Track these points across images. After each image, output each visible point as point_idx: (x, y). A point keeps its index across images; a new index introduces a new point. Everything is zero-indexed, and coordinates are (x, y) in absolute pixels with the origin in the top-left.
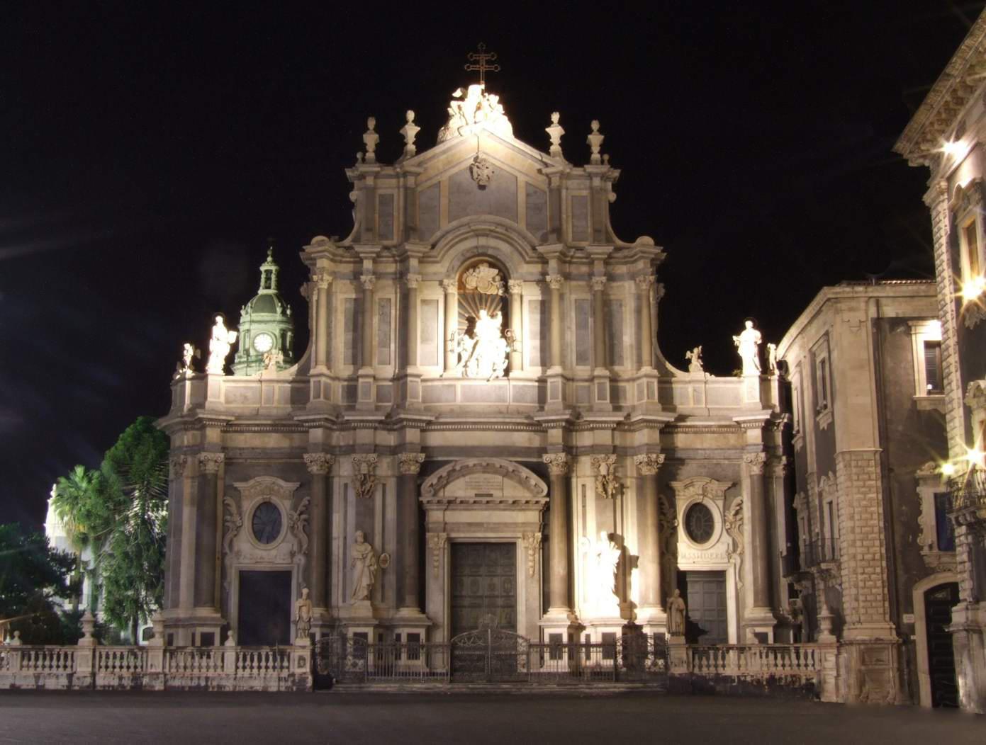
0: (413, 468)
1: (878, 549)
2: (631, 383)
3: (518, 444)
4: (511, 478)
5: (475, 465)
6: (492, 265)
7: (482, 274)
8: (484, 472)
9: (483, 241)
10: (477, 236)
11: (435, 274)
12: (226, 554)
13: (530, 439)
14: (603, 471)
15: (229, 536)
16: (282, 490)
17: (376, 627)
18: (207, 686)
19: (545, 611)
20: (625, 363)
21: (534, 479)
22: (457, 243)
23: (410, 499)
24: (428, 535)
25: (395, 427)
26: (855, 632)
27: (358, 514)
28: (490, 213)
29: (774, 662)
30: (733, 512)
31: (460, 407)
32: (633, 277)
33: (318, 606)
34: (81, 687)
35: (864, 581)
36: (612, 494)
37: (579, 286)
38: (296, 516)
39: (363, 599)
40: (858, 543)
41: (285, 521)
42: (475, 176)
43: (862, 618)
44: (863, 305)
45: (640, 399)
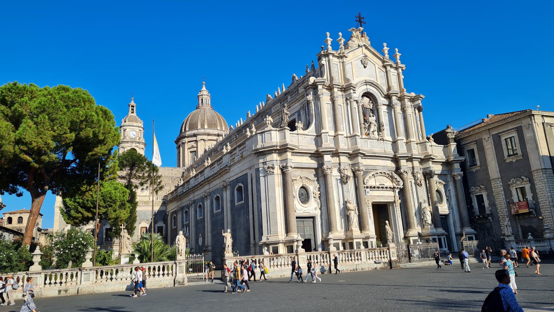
3: (389, 166)
5: (380, 173)
6: (367, 97)
7: (365, 100)
9: (369, 87)
10: (366, 85)
21: (399, 179)
28: (368, 77)
31: (371, 150)
41: (311, 195)
42: (363, 62)
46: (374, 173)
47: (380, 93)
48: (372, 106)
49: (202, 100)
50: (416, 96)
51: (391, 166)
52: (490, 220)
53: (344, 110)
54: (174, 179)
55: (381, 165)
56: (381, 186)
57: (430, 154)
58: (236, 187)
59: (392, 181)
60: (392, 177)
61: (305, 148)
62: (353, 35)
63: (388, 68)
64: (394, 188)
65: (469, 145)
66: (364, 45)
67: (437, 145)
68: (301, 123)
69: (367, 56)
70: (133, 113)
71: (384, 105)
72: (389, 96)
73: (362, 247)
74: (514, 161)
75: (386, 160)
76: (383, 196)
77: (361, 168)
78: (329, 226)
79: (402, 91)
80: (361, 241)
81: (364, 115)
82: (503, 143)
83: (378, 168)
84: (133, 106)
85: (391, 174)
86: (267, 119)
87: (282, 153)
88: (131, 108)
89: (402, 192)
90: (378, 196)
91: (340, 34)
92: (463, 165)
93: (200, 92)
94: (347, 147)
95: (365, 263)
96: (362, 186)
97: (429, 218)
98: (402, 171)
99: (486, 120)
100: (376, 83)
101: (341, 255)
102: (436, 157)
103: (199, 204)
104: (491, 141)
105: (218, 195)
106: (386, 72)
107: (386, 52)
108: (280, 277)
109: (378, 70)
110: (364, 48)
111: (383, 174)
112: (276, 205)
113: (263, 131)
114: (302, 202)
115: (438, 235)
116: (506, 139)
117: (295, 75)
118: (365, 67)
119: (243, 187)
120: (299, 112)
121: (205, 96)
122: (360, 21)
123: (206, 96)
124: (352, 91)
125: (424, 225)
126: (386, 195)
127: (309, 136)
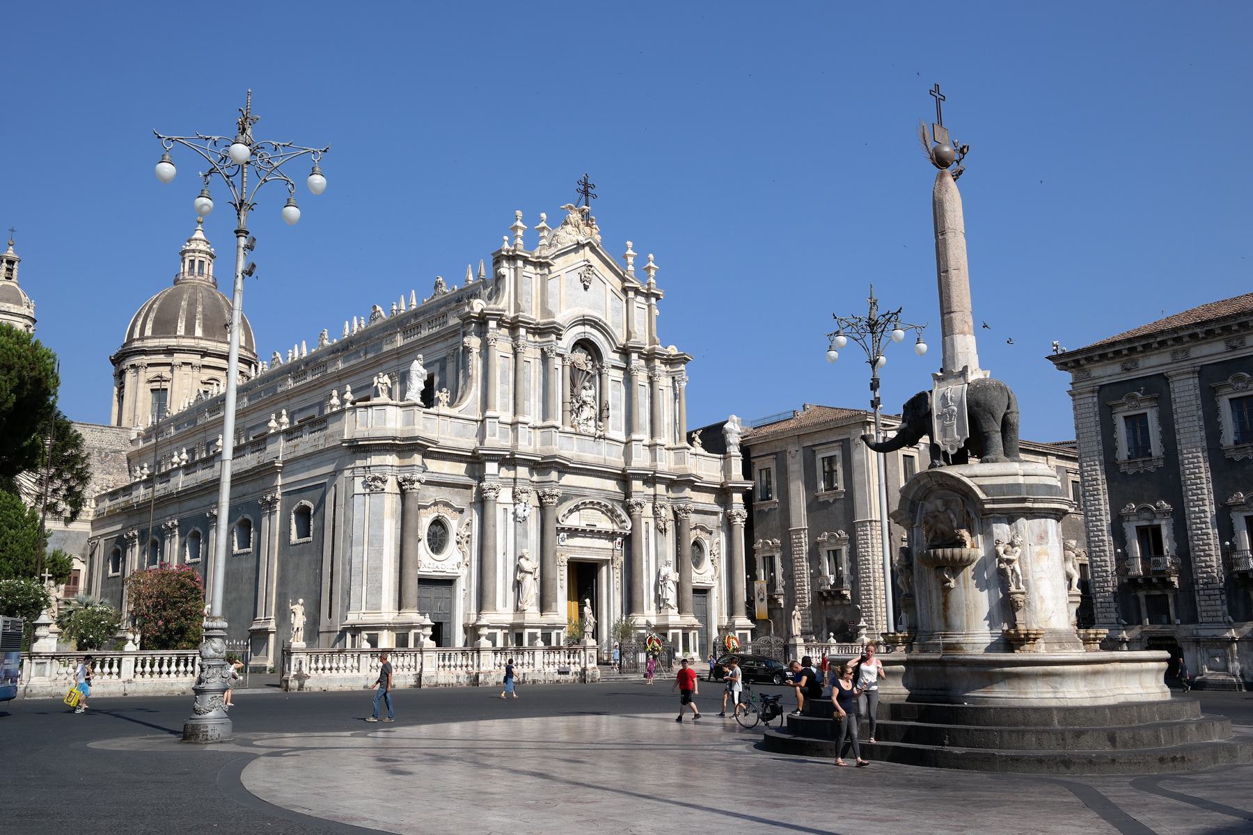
6: (584, 348)
9: (588, 329)
10: (584, 324)
18: (524, 682)
21: (624, 516)
25: (538, 467)
34: (429, 686)
41: (452, 538)
46: (578, 501)
47: (610, 343)
48: (590, 367)
49: (192, 262)
50: (677, 355)
52: (781, 604)
53: (535, 372)
54: (107, 455)
56: (588, 529)
57: (689, 472)
58: (294, 509)
59: (613, 521)
60: (612, 512)
61: (450, 444)
62: (568, 221)
63: (631, 294)
64: (614, 533)
65: (763, 458)
66: (589, 242)
67: (706, 453)
68: (447, 393)
69: (591, 266)
70: (11, 279)
71: (614, 367)
72: (626, 350)
73: (540, 643)
74: (831, 501)
77: (555, 492)
78: (482, 602)
79: (652, 342)
80: (539, 632)
81: (573, 385)
82: (819, 464)
83: (587, 494)
84: (11, 262)
85: (610, 507)
86: (381, 380)
87: (403, 451)
88: (5, 265)
89: (629, 541)
91: (544, 215)
92: (748, 497)
93: (189, 241)
94: (532, 447)
95: (539, 671)
96: (551, 526)
97: (671, 595)
98: (632, 501)
99: (801, 414)
100: (603, 322)
101: (499, 654)
102: (700, 478)
103: (192, 530)
104: (799, 457)
105: (247, 516)
106: (627, 302)
107: (630, 260)
109: (610, 295)
110: (587, 249)
111: (594, 505)
112: (381, 554)
113: (369, 403)
114: (432, 550)
115: (683, 629)
116: (823, 458)
117: (441, 279)
118: (586, 288)
119: (312, 508)
120: (443, 362)
121: (200, 255)
122: (586, 193)
123: (205, 255)
124: (553, 337)
125: (660, 608)
127: (461, 421)
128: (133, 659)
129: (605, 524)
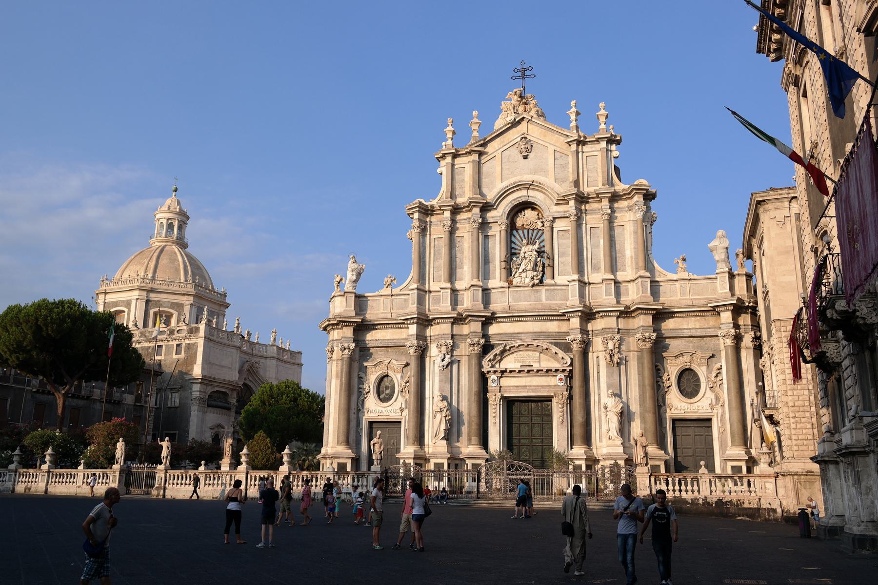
0: (476, 348)
1: (807, 397)
2: (632, 283)
3: (550, 330)
4: (546, 354)
5: (519, 345)
8: (526, 350)
9: (524, 193)
11: (493, 217)
12: (360, 410)
13: (559, 326)
14: (611, 346)
15: (362, 398)
16: (395, 367)
17: (449, 459)
19: (572, 448)
20: (627, 269)
21: (561, 354)
22: (507, 195)
23: (475, 370)
24: (489, 395)
26: (789, 465)
27: (440, 381)
28: (530, 174)
29: (672, 488)
30: (715, 374)
32: (630, 209)
33: (413, 444)
35: (796, 423)
36: (617, 363)
37: (593, 218)
38: (403, 384)
39: (442, 439)
40: (790, 393)
43: (796, 454)
44: (787, 204)
45: (637, 295)
51: (557, 330)
55: (531, 330)
64: (548, 371)
75: (544, 321)
76: (526, 386)
90: (542, 386)
108: (212, 499)
126: (535, 384)
128: (83, 474)
129: (547, 363)
